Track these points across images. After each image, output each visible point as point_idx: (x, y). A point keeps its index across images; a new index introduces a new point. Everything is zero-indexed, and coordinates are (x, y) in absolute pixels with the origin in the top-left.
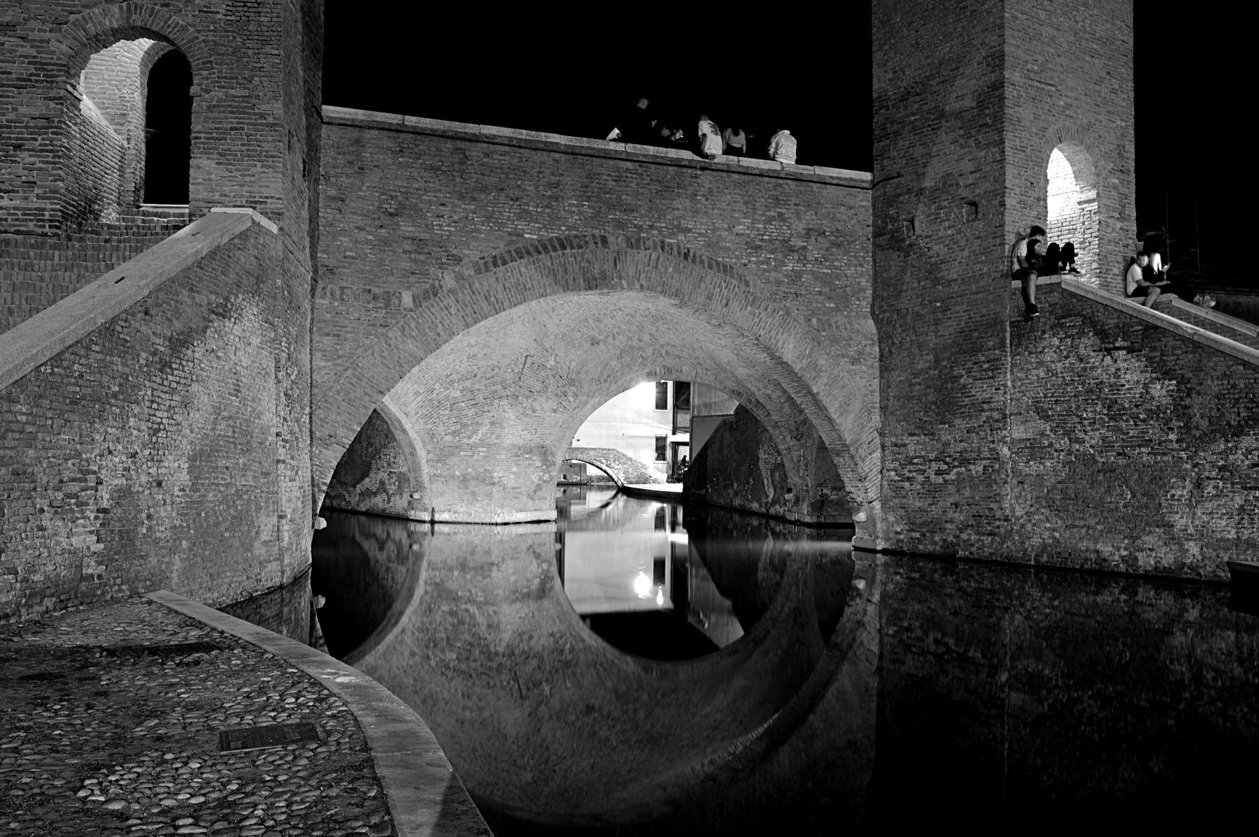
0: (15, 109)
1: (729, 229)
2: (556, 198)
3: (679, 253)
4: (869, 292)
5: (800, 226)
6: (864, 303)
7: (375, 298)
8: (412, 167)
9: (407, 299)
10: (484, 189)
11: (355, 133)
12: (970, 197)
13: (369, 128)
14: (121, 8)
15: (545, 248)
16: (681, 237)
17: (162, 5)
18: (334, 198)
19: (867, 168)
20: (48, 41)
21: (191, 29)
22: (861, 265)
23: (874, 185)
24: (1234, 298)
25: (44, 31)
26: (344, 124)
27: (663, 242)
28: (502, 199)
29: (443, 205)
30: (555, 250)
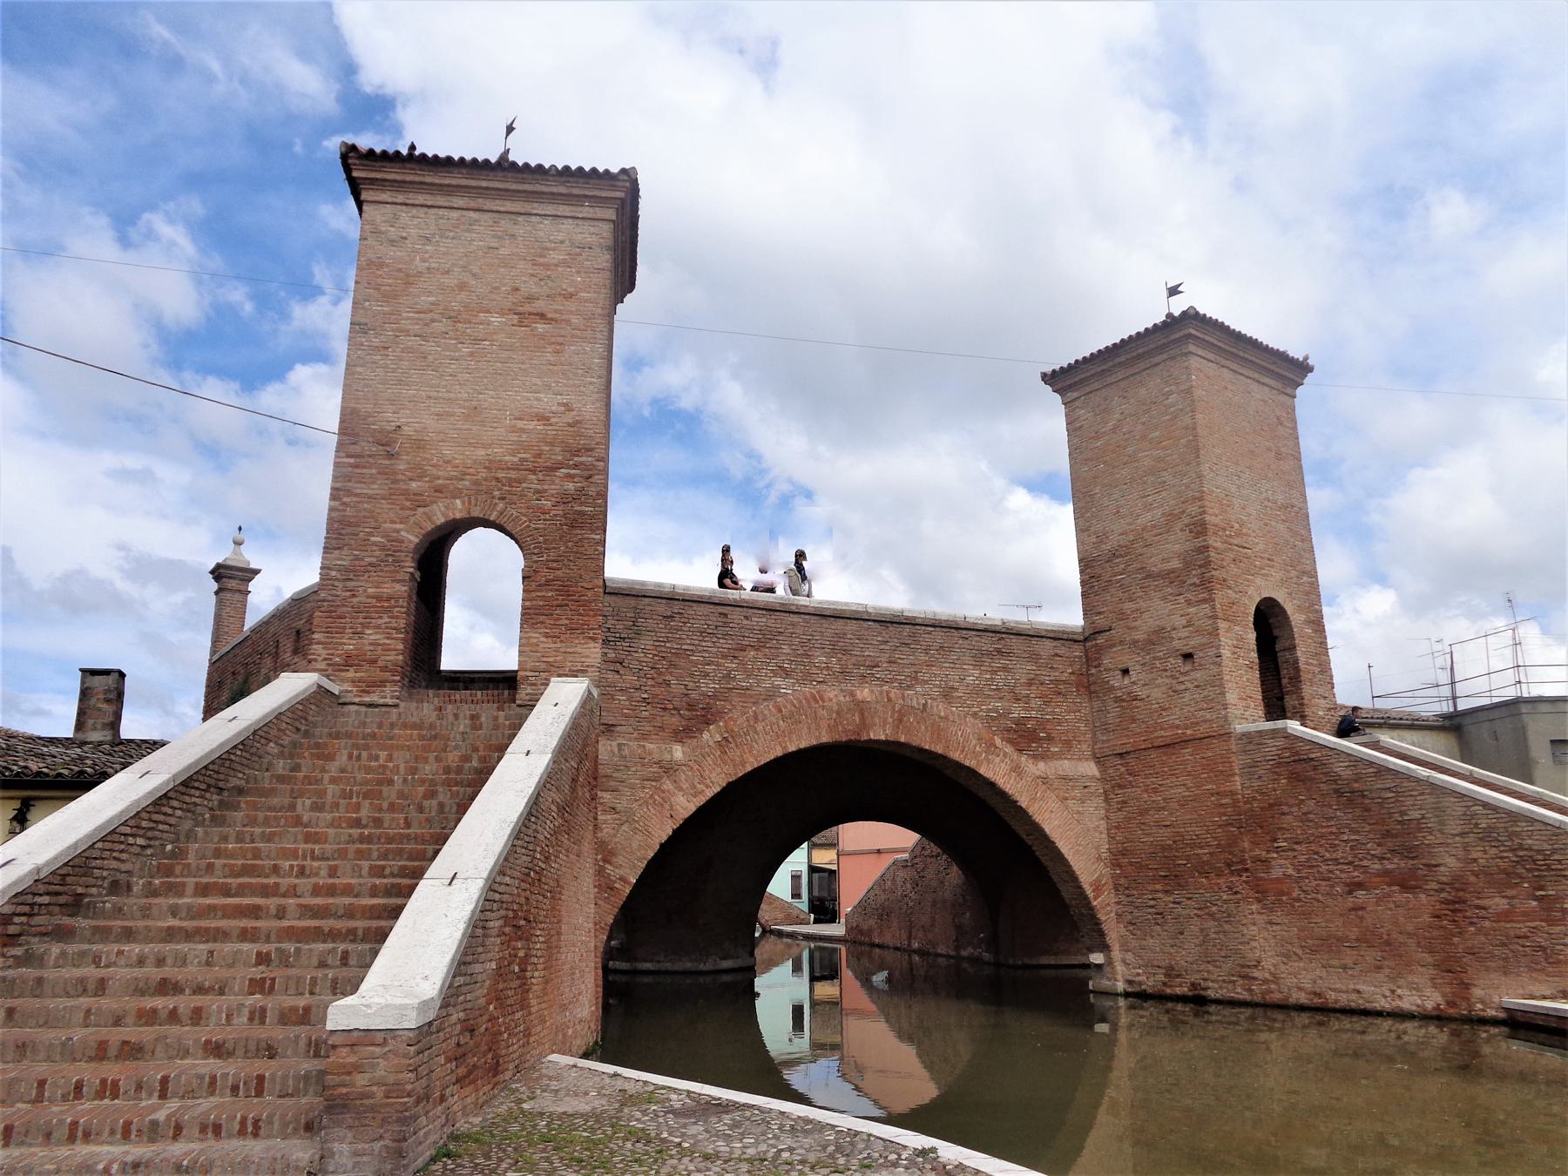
0: (365, 591)
3: (918, 704)
6: (1084, 747)
8: (681, 630)
12: (1186, 650)
13: (645, 596)
14: (463, 503)
17: (499, 499)
20: (398, 531)
21: (524, 519)
22: (1079, 711)
25: (393, 522)
28: (760, 655)
29: (709, 665)
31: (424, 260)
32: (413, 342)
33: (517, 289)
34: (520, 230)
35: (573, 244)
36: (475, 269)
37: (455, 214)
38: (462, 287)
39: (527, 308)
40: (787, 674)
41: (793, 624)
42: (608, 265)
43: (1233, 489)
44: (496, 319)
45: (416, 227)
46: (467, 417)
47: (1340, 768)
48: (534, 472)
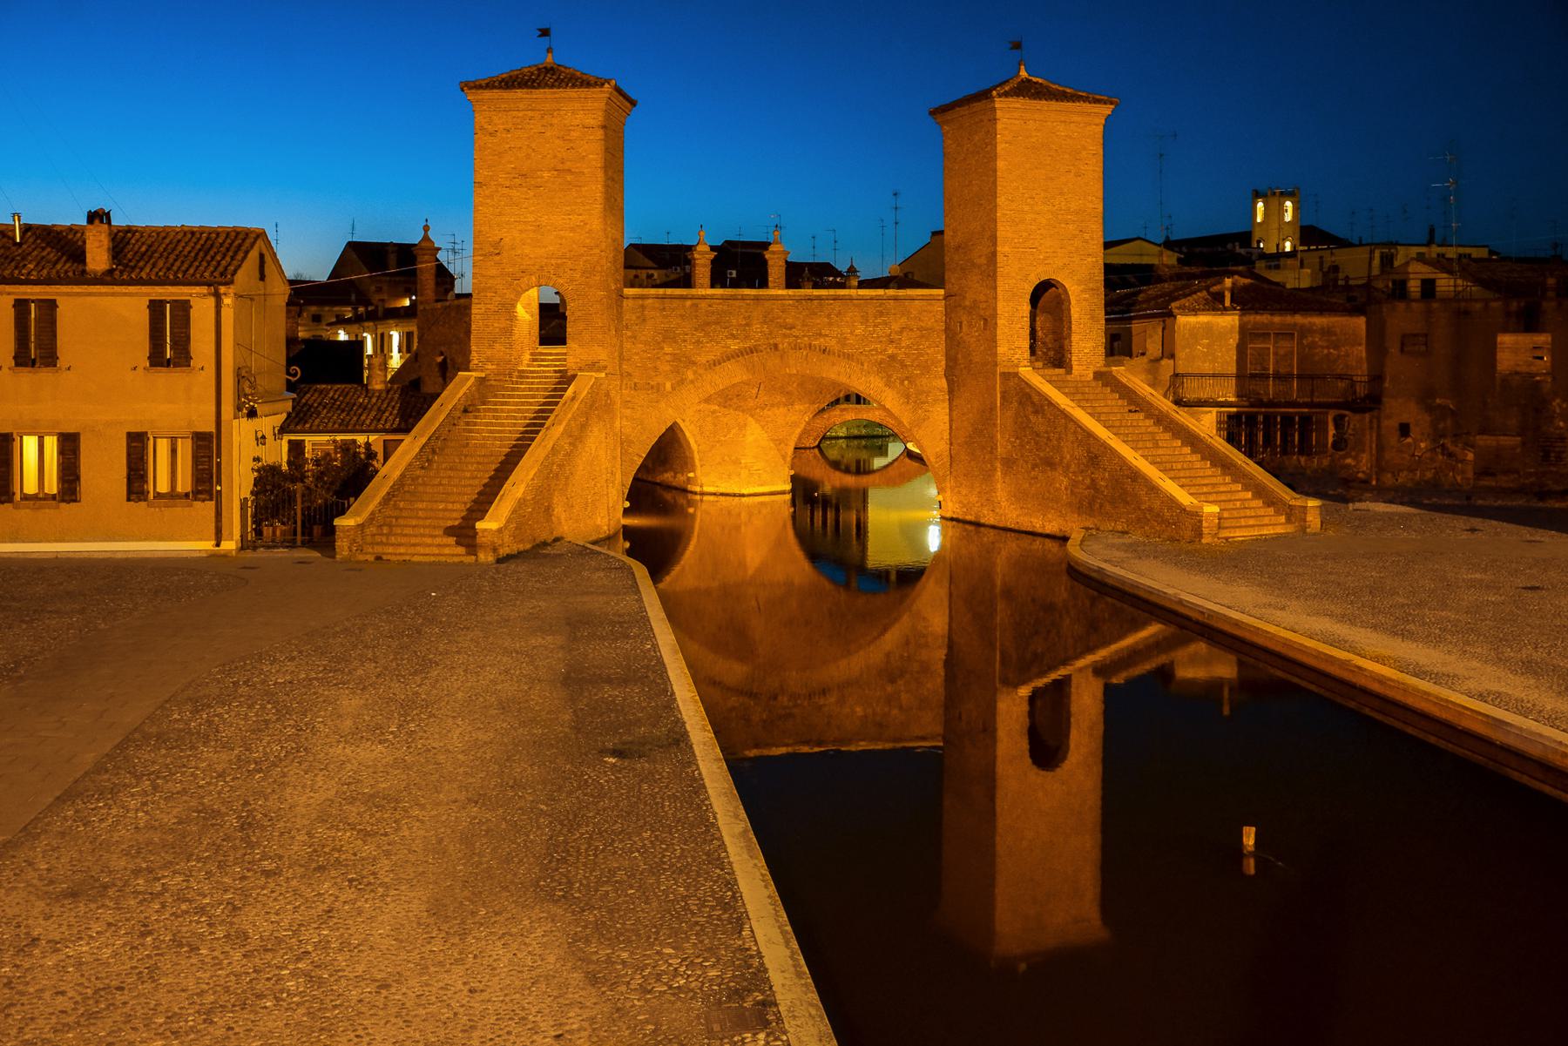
1: (851, 333)
2: (747, 325)
4: (944, 362)
5: (896, 327)
7: (652, 387)
9: (668, 386)
10: (708, 324)
11: (640, 302)
15: (742, 354)
16: (822, 340)
18: (630, 337)
19: (940, 285)
23: (946, 297)
24: (1309, 319)
26: (636, 298)
27: (810, 345)
30: (747, 354)
31: (507, 143)
32: (506, 191)
33: (555, 157)
34: (555, 121)
35: (584, 127)
36: (533, 145)
37: (520, 114)
38: (528, 156)
39: (560, 167)
40: (734, 337)
41: (739, 307)
42: (603, 137)
43: (1026, 208)
44: (546, 174)
45: (503, 124)
46: (534, 231)
47: (1036, 399)
48: (570, 259)
